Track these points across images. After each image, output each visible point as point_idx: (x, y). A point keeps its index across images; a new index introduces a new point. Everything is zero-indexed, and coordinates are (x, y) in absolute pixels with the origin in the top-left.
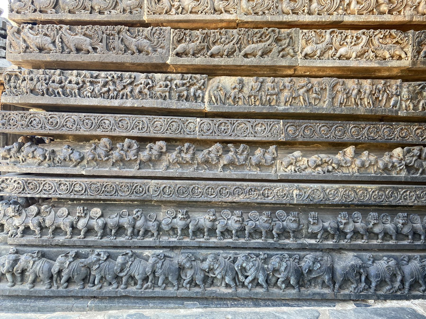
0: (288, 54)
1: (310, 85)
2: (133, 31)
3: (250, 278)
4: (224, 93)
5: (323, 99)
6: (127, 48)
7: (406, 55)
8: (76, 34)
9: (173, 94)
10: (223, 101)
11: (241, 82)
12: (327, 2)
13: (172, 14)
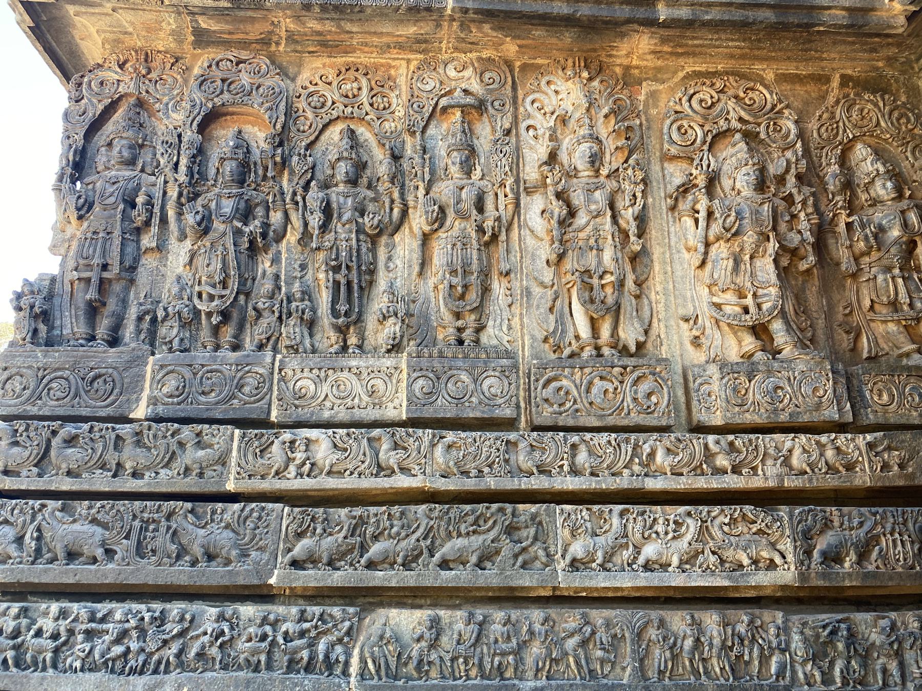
0: (536, 558)
1: (588, 629)
2: (201, 510)
4: (395, 650)
6: (185, 550)
7: (784, 557)
8: (74, 521)
9: (277, 655)
10: (394, 670)
11: (435, 623)
12: (608, 451)
13: (288, 476)
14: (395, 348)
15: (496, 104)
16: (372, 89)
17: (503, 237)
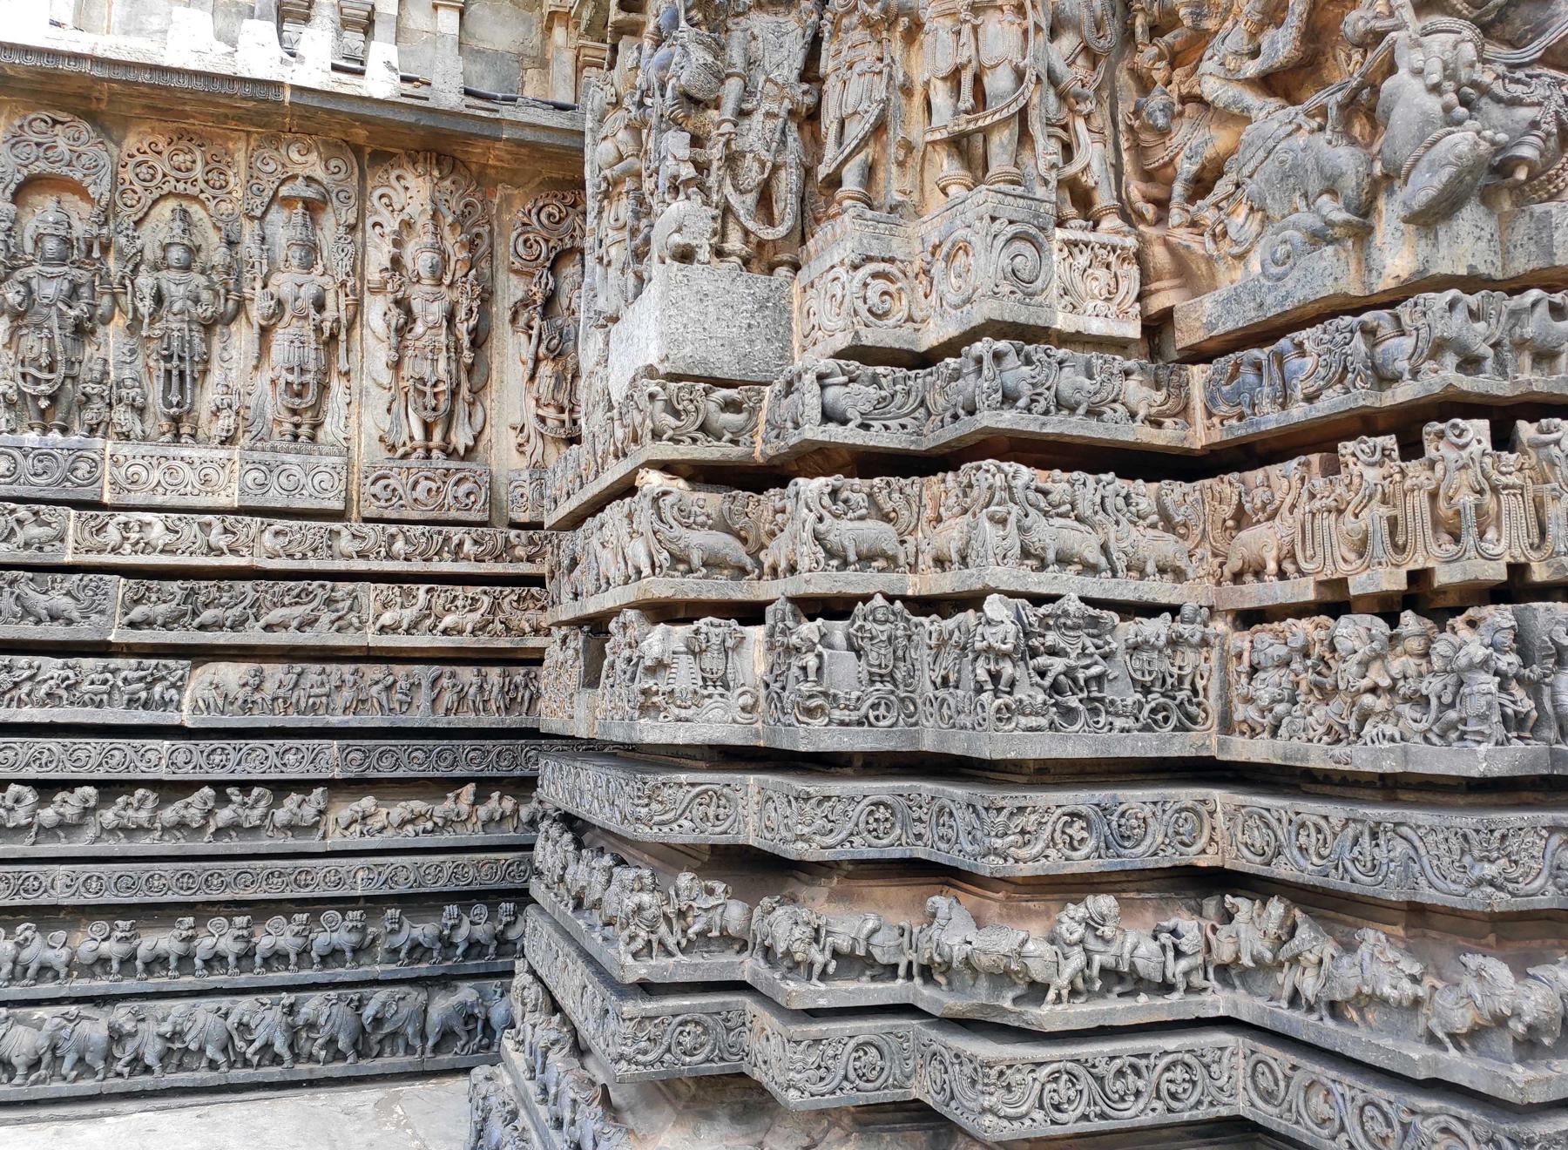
0: (351, 624)
1: (391, 679)
3: (257, 1045)
5: (415, 702)
9: (116, 696)
14: (229, 440)
15: (342, 195)
16: (207, 163)
17: (342, 336)
